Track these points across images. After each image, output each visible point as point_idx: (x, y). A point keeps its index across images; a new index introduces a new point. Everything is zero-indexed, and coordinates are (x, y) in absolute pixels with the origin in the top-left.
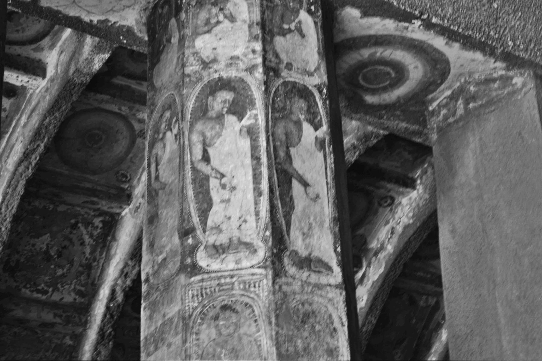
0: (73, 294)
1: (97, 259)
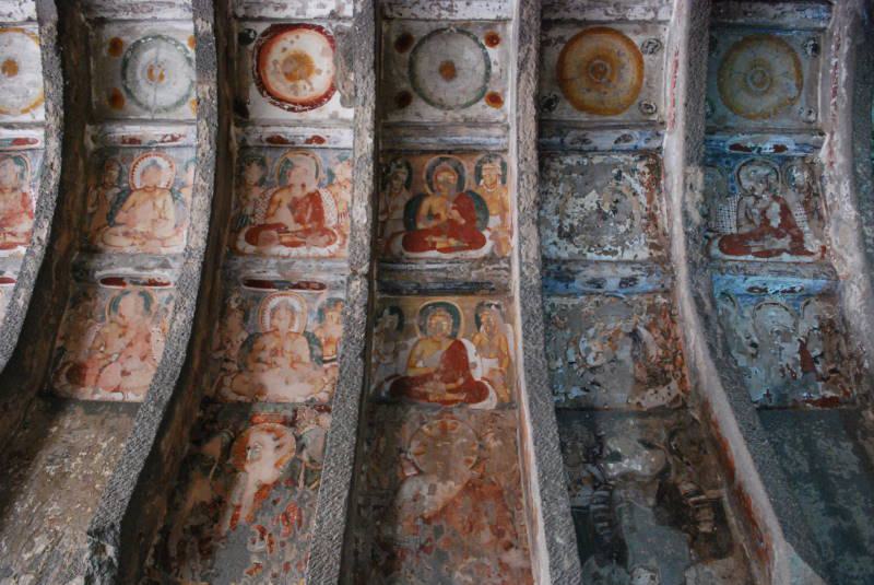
0: (646, 249)
1: (658, 205)
